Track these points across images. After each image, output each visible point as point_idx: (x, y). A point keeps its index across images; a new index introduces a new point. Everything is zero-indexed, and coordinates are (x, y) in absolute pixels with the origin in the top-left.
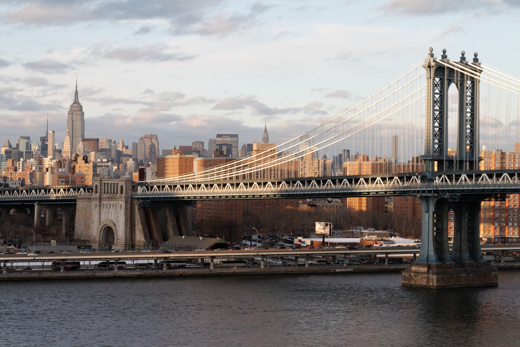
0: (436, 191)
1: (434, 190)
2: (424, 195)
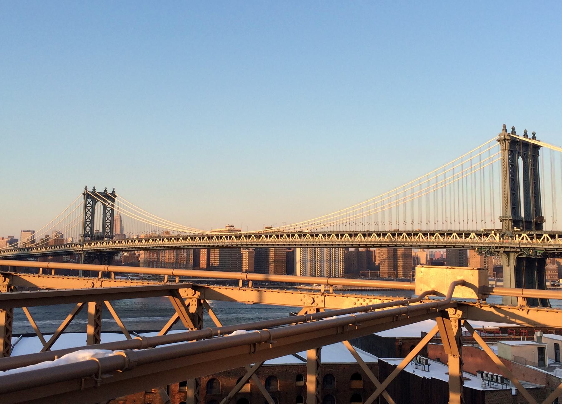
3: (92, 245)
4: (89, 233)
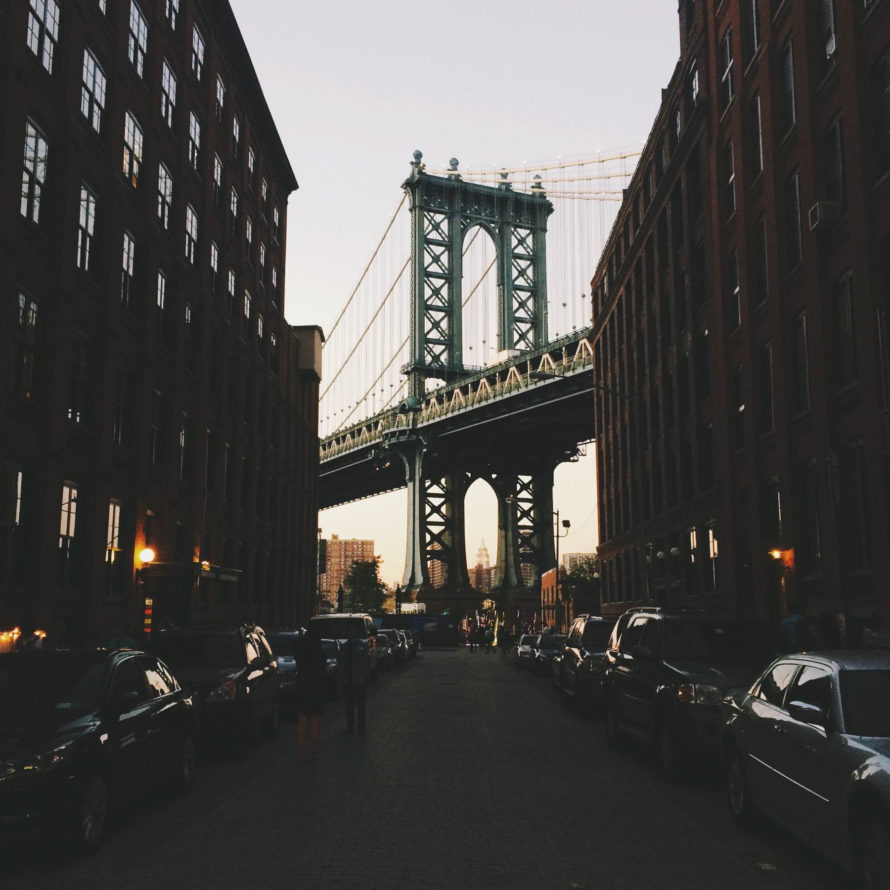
4: (444, 358)
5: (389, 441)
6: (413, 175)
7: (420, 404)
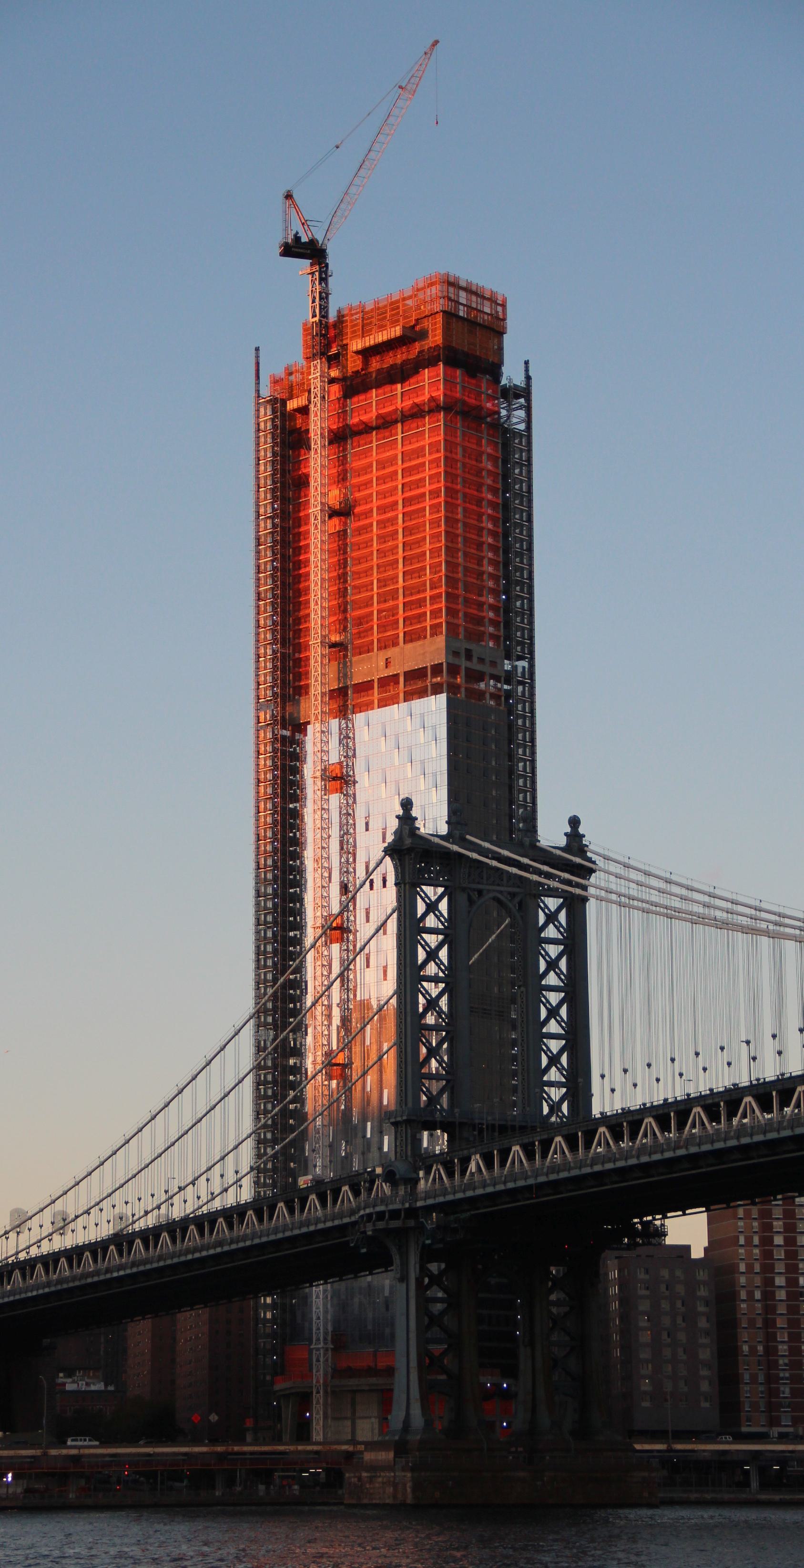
0: (412, 1212)
1: (406, 1210)
2: (381, 1225)
3: (473, 1167)
5: (374, 1225)
6: (398, 833)
7: (416, 1171)
